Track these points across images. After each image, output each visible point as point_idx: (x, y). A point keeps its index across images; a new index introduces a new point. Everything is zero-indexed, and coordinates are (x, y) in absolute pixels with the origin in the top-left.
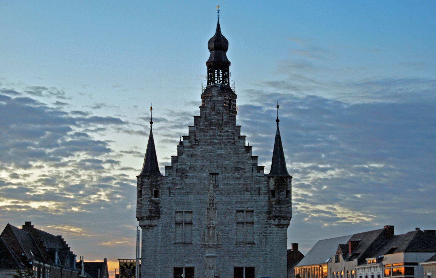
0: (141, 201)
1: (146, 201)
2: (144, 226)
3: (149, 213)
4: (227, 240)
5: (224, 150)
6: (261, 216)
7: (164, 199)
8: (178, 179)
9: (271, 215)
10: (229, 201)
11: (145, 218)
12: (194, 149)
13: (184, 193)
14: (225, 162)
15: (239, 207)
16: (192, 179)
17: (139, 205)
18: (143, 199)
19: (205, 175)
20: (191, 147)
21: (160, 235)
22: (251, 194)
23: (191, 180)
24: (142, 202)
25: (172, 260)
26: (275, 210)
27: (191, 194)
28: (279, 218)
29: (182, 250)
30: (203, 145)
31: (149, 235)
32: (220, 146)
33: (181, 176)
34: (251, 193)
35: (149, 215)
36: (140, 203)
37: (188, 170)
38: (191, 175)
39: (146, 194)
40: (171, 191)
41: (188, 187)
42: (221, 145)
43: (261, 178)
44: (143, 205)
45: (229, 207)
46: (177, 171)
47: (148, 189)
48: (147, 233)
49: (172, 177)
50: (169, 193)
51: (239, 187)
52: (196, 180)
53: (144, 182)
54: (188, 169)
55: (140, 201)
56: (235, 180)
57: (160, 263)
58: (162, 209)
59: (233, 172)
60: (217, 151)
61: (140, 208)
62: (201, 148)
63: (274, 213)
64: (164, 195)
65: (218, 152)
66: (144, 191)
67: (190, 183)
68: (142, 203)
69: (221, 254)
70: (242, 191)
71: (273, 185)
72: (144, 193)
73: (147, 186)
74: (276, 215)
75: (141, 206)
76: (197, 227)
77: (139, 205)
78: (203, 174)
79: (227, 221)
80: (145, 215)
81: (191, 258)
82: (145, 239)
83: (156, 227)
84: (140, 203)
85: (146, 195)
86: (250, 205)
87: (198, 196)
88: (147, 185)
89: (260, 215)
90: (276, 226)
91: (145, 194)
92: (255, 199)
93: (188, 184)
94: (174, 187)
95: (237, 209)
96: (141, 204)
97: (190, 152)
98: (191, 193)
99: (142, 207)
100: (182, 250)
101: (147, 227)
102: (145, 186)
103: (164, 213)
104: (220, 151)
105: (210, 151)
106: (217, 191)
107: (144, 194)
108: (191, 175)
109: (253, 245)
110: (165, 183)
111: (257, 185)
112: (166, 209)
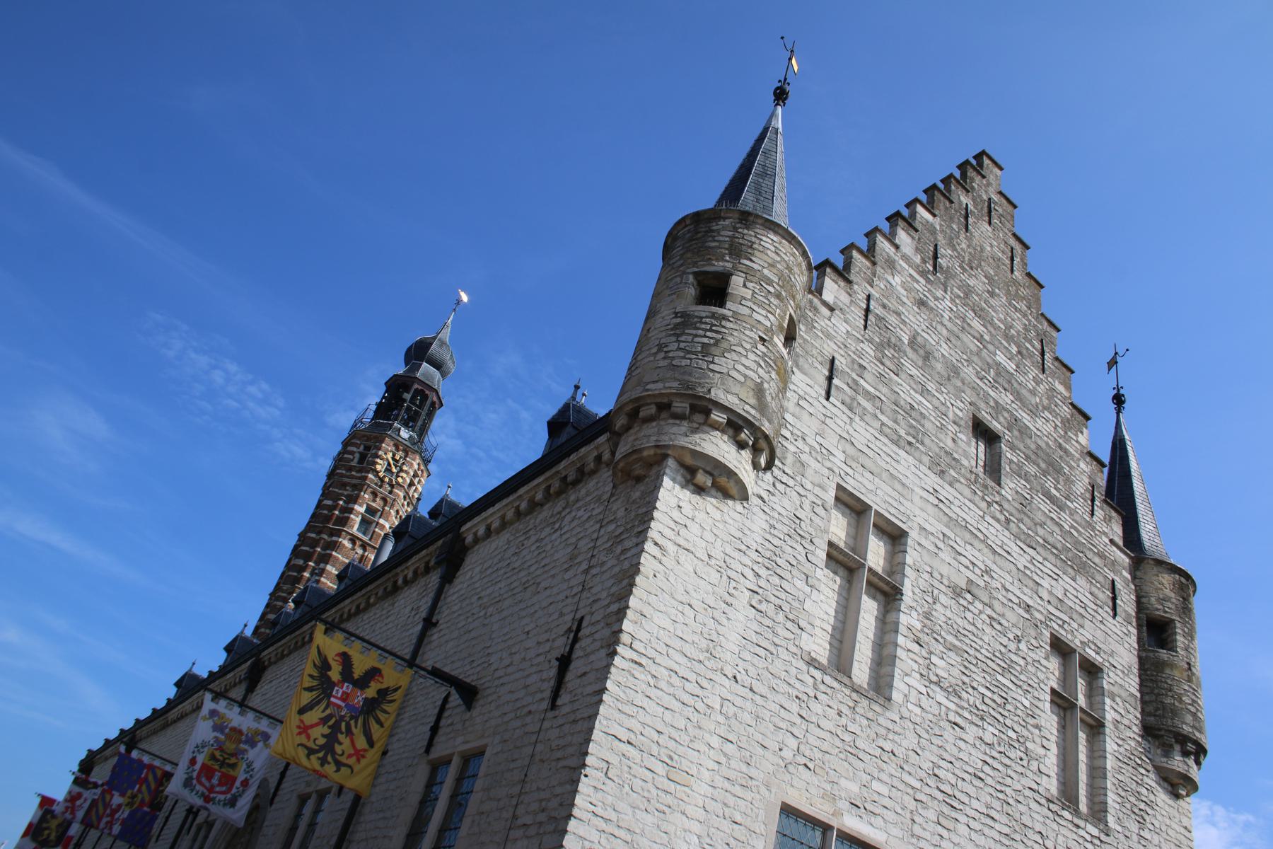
0: (715, 318)
1: (747, 332)
2: (689, 460)
3: (752, 401)
4: (1021, 759)
5: (1017, 367)
6: (1120, 703)
7: (802, 393)
8: (869, 349)
10: (1028, 572)
11: (719, 417)
12: (929, 287)
13: (883, 424)
14: (1020, 411)
15: (1060, 623)
16: (916, 392)
17: (696, 336)
18: (729, 313)
19: (960, 410)
20: (923, 274)
21: (750, 564)
22: (1091, 593)
23: (912, 392)
25: (784, 753)
27: (908, 448)
28: (1191, 747)
29: (840, 714)
30: (959, 297)
31: (694, 528)
32: (1006, 345)
33: (880, 347)
34: (1094, 589)
35: (753, 412)
37: (903, 343)
38: (914, 372)
39: (754, 303)
40: (835, 381)
41: (903, 413)
42: (1010, 345)
43: (1115, 549)
44: (724, 345)
45: (1030, 602)
46: (866, 316)
47: (772, 290)
48: (687, 509)
49: (844, 324)
50: (824, 383)
51: (1059, 537)
52: (931, 407)
53: (755, 246)
54: (906, 342)
55: (708, 320)
56: (1048, 502)
57: (715, 741)
58: (788, 435)
59: (1043, 465)
60: (998, 352)
61: (699, 349)
62: (952, 300)
64: (805, 374)
65: (1001, 358)
66: (750, 285)
67: (909, 400)
69: (997, 826)
70: (1069, 563)
72: (748, 294)
73: (766, 272)
74: (1184, 726)
75: (712, 341)
76: (918, 626)
77: (696, 336)
78: (952, 402)
79: (1022, 662)
80: (730, 400)
81: (876, 785)
82: (669, 542)
83: (738, 507)
84: (703, 329)
85: (755, 307)
86: (1091, 638)
87: (932, 480)
88: (766, 265)
89: (1118, 700)
90: (1165, 779)
92: (1105, 622)
93: (902, 403)
94: (849, 371)
95: (1056, 627)
96: (709, 334)
97: (916, 285)
98: (910, 443)
99: (714, 350)
100: (840, 714)
101: (701, 478)
102: (756, 266)
103: (790, 459)
104: (1005, 358)
105: (978, 336)
106: (995, 505)
107: (745, 299)
108: (914, 372)
109: (1103, 837)
110: (816, 325)
111: (1105, 569)
112: (800, 444)
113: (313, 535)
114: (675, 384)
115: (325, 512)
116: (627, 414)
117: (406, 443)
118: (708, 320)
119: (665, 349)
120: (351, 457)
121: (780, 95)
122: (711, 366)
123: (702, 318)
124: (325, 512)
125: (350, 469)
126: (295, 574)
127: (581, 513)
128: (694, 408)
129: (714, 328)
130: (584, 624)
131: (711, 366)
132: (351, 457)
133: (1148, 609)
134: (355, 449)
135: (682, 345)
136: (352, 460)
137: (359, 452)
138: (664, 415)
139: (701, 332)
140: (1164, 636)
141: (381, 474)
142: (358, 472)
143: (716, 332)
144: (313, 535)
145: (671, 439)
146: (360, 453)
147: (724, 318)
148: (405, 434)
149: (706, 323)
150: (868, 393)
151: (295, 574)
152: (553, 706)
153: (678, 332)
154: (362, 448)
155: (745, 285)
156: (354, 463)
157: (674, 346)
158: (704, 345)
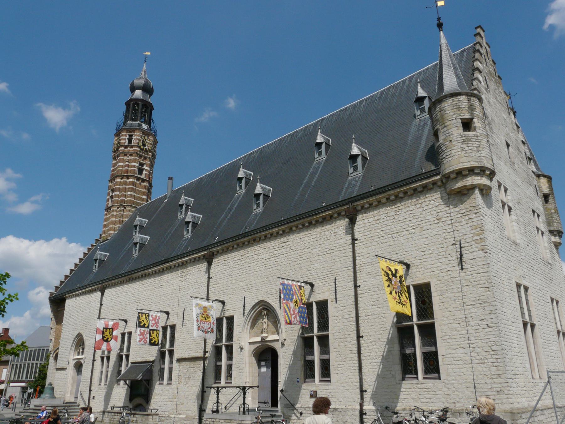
2: (482, 187)
9: (552, 228)
17: (473, 144)
18: (478, 134)
24: (478, 139)
26: (556, 221)
36: (475, 140)
61: (476, 149)
63: (557, 225)
68: (479, 141)
71: (546, 187)
75: (477, 146)
77: (473, 144)
91: (480, 126)
96: (477, 143)
99: (480, 149)
101: (484, 192)
107: (480, 127)
113: (119, 180)
114: (474, 163)
115: (121, 169)
116: (456, 173)
117: (147, 131)
118: (473, 138)
119: (464, 150)
120: (124, 141)
121: (440, 26)
122: (482, 155)
123: (471, 137)
124: (121, 169)
125: (126, 147)
126: (117, 199)
127: (432, 202)
128: (481, 171)
129: (477, 140)
130: (462, 242)
131: (482, 155)
132: (124, 141)
133: (543, 191)
134: (124, 137)
135: (470, 148)
136: (125, 143)
137: (127, 139)
138: (471, 173)
139: (474, 143)
140: (547, 199)
141: (142, 147)
142: (130, 148)
143: (477, 142)
144: (119, 180)
145: (477, 182)
146: (127, 139)
147: (477, 136)
148: (145, 126)
149: (474, 139)
150: (492, 144)
151: (117, 199)
152: (462, 269)
153: (466, 143)
154: (128, 137)
155: (478, 122)
156: (126, 144)
157: (467, 149)
158: (476, 147)
